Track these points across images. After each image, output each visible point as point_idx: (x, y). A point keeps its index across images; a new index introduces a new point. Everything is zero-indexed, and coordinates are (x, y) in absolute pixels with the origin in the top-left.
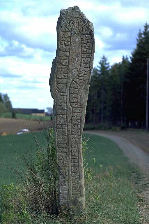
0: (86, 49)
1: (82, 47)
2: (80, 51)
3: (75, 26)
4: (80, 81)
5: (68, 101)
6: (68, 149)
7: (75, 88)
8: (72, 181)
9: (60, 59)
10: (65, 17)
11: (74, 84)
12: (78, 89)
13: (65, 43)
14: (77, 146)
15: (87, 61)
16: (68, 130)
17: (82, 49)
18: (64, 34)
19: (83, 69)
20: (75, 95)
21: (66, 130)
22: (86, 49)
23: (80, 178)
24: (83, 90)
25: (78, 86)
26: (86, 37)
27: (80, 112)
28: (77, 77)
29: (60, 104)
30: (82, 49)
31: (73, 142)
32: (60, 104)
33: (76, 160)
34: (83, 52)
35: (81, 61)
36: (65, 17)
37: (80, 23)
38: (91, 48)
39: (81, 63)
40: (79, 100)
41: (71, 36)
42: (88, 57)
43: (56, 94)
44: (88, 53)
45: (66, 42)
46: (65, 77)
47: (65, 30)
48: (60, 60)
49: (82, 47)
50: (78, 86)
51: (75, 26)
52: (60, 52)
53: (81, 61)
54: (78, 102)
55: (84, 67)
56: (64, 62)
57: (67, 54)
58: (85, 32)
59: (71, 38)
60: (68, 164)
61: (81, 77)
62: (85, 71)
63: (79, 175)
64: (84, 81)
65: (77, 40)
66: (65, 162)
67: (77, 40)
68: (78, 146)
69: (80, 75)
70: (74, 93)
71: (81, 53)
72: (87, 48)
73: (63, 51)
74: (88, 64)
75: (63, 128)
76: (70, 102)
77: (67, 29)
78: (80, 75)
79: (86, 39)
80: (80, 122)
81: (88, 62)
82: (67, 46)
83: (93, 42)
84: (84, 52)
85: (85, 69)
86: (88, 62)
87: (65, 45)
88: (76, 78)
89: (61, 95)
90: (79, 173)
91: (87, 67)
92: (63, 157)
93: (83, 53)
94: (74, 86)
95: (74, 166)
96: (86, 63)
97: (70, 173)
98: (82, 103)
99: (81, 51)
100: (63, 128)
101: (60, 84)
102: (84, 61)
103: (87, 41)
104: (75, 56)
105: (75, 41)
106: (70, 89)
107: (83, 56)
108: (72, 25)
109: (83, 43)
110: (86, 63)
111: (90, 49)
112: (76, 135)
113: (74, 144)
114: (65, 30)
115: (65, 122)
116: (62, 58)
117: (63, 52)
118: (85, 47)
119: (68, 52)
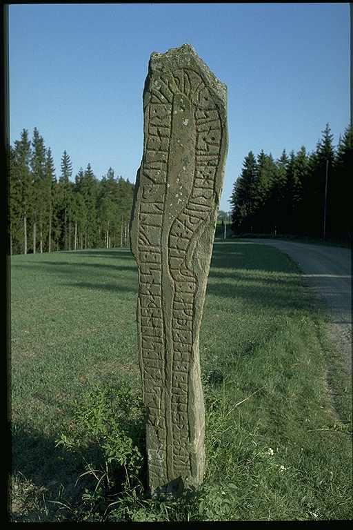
0: (208, 143)
3: (183, 89)
6: (166, 373)
8: (173, 455)
9: (147, 169)
10: (159, 69)
12: (188, 238)
13: (158, 132)
14: (185, 368)
15: (210, 172)
16: (165, 332)
19: (199, 192)
20: (182, 251)
21: (162, 330)
22: (208, 143)
23: (191, 436)
24: (201, 240)
25: (187, 233)
26: (207, 117)
27: (192, 291)
29: (148, 272)
31: (176, 358)
32: (148, 272)
33: (184, 398)
34: (199, 152)
36: (159, 69)
38: (219, 142)
39: (196, 177)
40: (190, 264)
41: (172, 114)
42: (211, 165)
43: (139, 248)
44: (210, 155)
47: (159, 101)
48: (147, 171)
50: (187, 233)
51: (183, 89)
52: (148, 152)
54: (187, 268)
55: (202, 188)
57: (165, 156)
58: (204, 104)
60: (166, 404)
61: (193, 210)
62: (203, 196)
63: (189, 432)
64: (201, 221)
68: (187, 367)
70: (178, 248)
71: (196, 154)
72: (210, 140)
73: (154, 150)
74: (211, 179)
75: (154, 326)
79: (208, 119)
80: (191, 314)
82: (164, 136)
83: (223, 129)
87: (160, 135)
90: (189, 427)
91: (210, 188)
92: (155, 388)
93: (201, 155)
95: (179, 409)
98: (195, 271)
99: (197, 149)
100: (154, 326)
101: (148, 227)
102: (201, 172)
103: (209, 124)
107: (201, 161)
108: (175, 88)
109: (199, 130)
111: (216, 144)
112: (183, 342)
113: (178, 362)
115: (159, 311)
116: (152, 165)
117: (154, 152)
119: (166, 151)
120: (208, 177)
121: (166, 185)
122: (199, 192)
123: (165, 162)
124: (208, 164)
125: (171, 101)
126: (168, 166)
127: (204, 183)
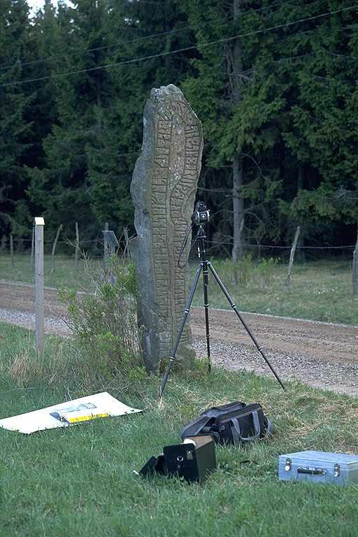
4: (185, 188)
5: (168, 216)
7: (177, 198)
11: (176, 192)
22: (192, 144)
26: (192, 129)
28: (181, 183)
37: (183, 109)
45: (165, 136)
49: (186, 142)
57: (167, 151)
58: (191, 122)
65: (179, 133)
66: (166, 299)
67: (179, 133)
76: (171, 217)
77: (166, 117)
81: (195, 163)
85: (192, 172)
86: (195, 163)
89: (159, 208)
94: (177, 195)
96: (192, 164)
97: (173, 314)
103: (193, 134)
106: (171, 200)
110: (192, 164)
118: (190, 142)
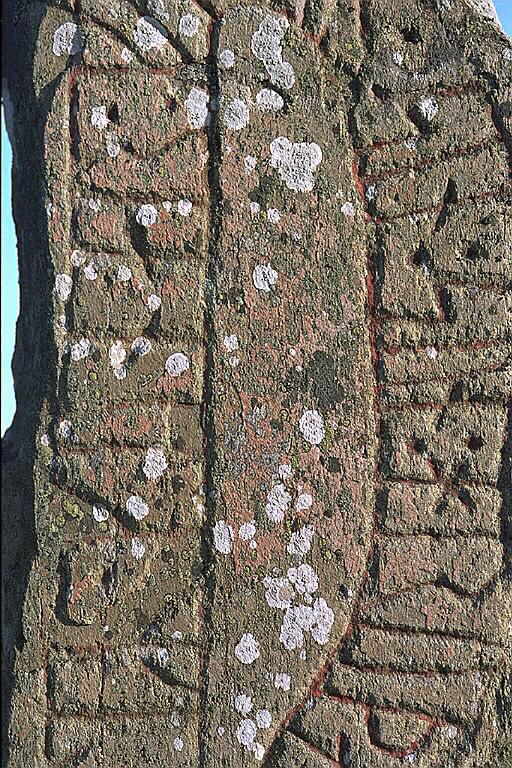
1: (377, 262)
2: (355, 311)
13: (137, 232)
15: (475, 443)
17: (376, 285)
18: (113, 114)
26: (426, 128)
28: (346, 678)
30: (376, 285)
35: (386, 451)
41: (213, 132)
45: (148, 214)
46: (172, 681)
47: (126, 56)
49: (377, 262)
53: (386, 451)
56: (141, 476)
59: (214, 147)
62: (442, 581)
64: (451, 731)
69: (366, 650)
71: (378, 342)
73: (115, 334)
78: (376, 644)
84: (414, 331)
88: (334, 693)
91: (479, 532)
102: (418, 446)
104: (294, 383)
105: (267, 188)
107: (411, 380)
109: (387, 204)
114: (126, 56)
120: (462, 469)
121: (206, 532)
122: (413, 558)
123: (188, 402)
124: (455, 395)
125: (200, 51)
126: (209, 430)
127: (441, 507)
